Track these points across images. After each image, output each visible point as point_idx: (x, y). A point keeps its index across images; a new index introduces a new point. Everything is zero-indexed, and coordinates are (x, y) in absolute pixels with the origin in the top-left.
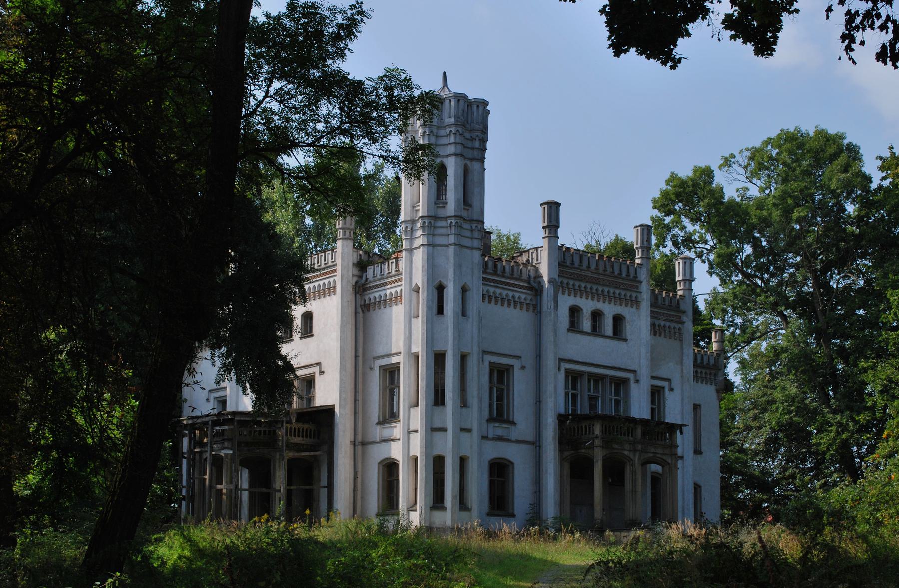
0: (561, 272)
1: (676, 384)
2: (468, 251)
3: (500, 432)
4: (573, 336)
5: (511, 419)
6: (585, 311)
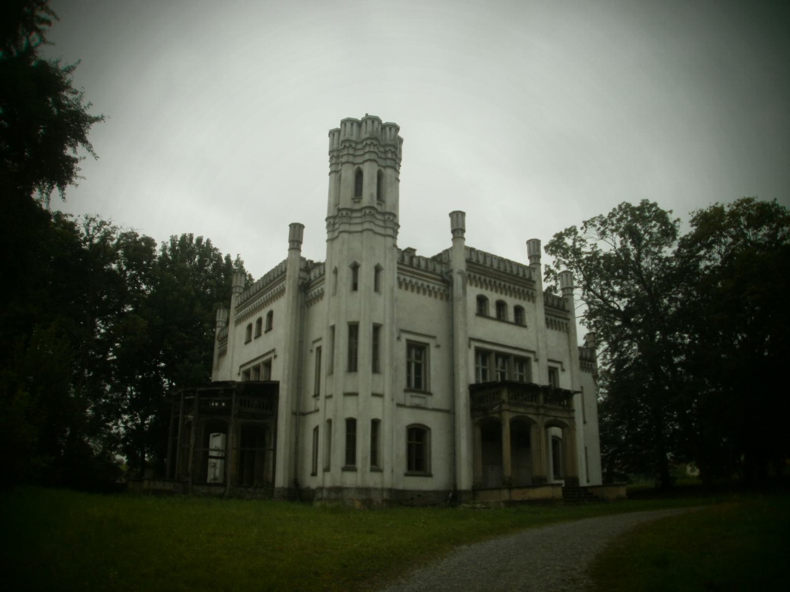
0: (468, 266)
2: (381, 238)
3: (417, 401)
5: (428, 391)
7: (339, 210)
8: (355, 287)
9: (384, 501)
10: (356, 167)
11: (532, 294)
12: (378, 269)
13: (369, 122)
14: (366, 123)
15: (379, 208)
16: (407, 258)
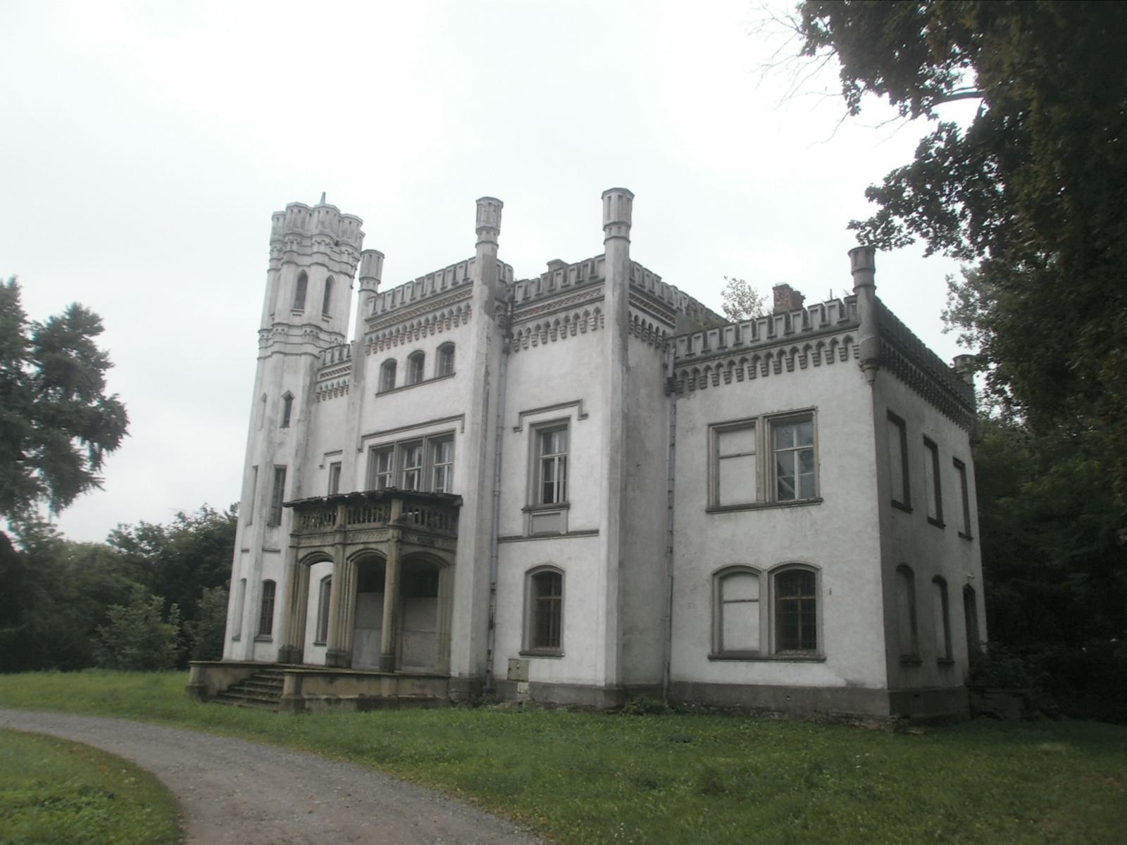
10: (301, 269)
15: (324, 326)
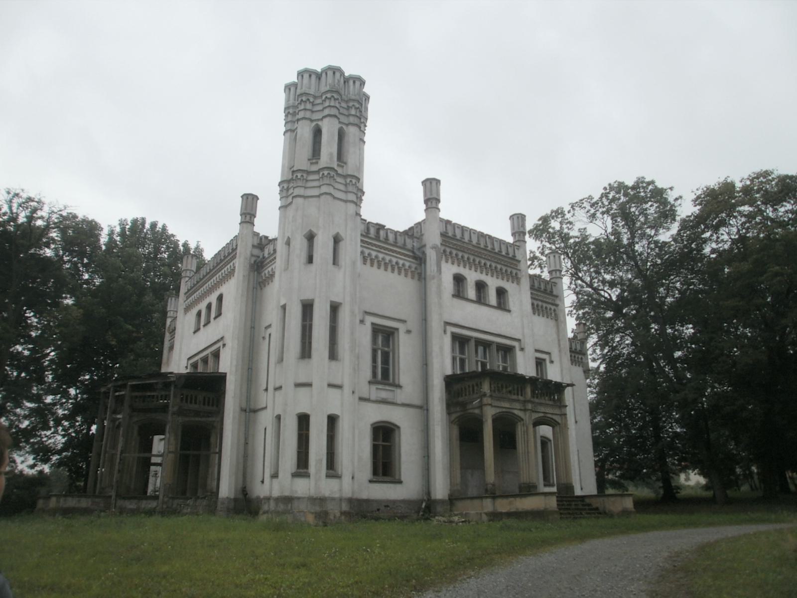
0: (443, 241)
1: (555, 356)
2: (342, 204)
3: (384, 395)
4: (458, 302)
5: (397, 382)
6: (469, 279)
7: (293, 172)
8: (310, 260)
9: (343, 513)
10: (314, 124)
11: (516, 274)
12: (337, 240)
13: (330, 73)
14: (326, 74)
15: (340, 171)
16: (372, 231)
